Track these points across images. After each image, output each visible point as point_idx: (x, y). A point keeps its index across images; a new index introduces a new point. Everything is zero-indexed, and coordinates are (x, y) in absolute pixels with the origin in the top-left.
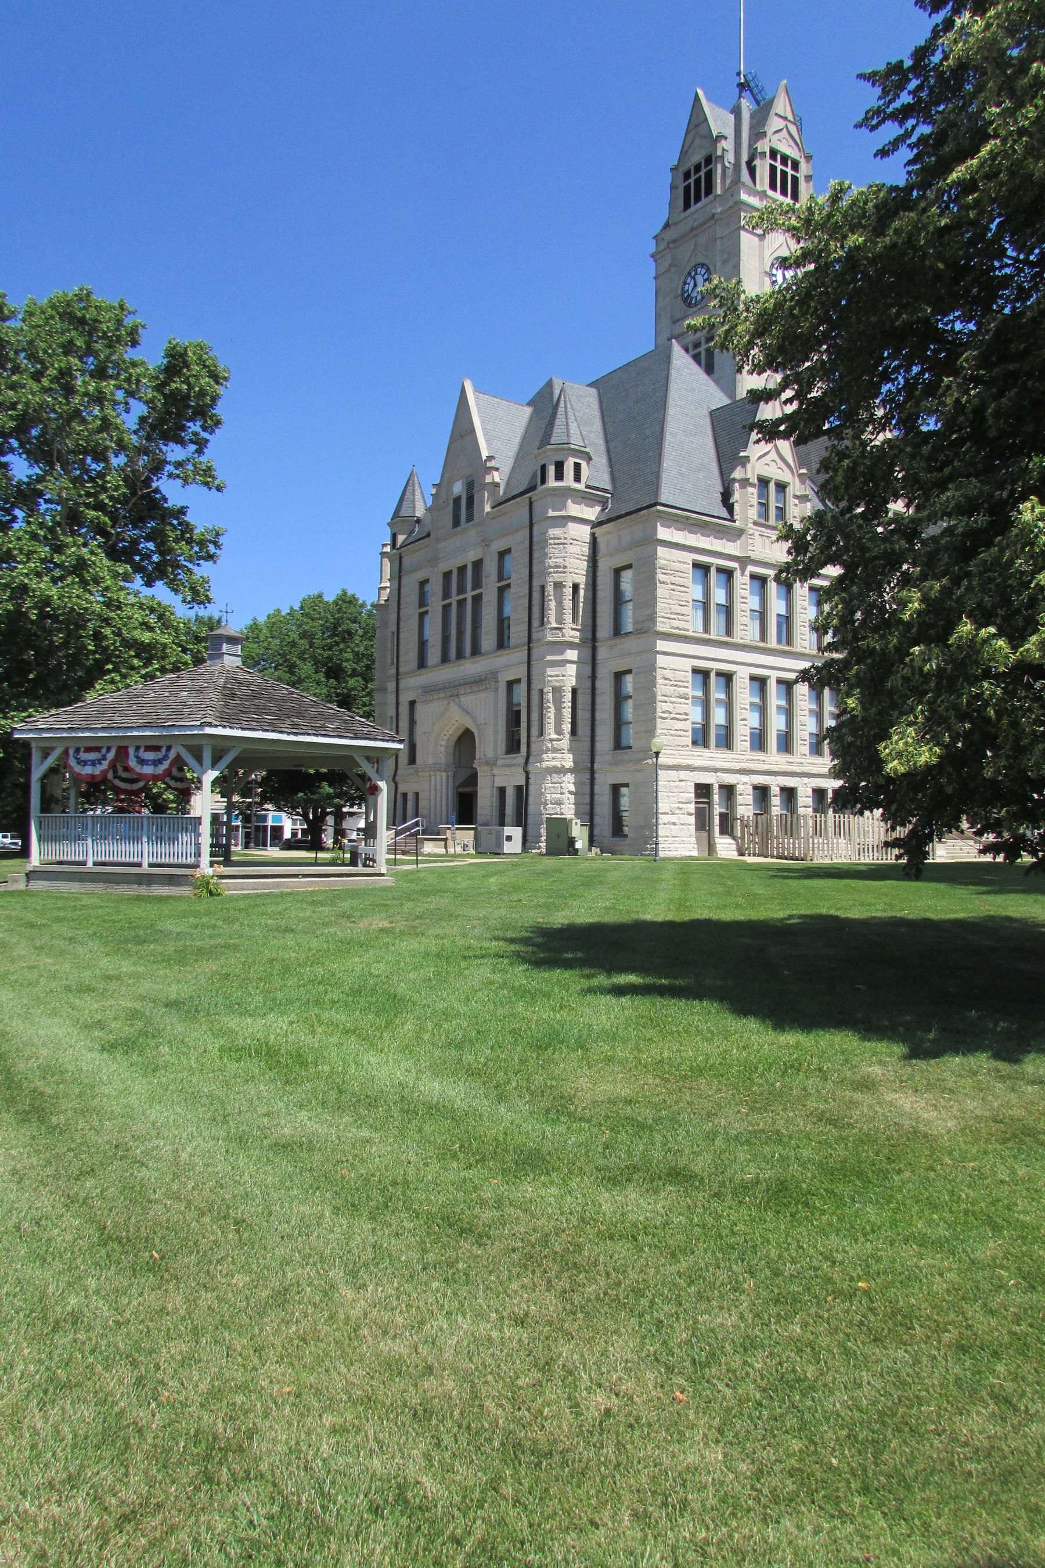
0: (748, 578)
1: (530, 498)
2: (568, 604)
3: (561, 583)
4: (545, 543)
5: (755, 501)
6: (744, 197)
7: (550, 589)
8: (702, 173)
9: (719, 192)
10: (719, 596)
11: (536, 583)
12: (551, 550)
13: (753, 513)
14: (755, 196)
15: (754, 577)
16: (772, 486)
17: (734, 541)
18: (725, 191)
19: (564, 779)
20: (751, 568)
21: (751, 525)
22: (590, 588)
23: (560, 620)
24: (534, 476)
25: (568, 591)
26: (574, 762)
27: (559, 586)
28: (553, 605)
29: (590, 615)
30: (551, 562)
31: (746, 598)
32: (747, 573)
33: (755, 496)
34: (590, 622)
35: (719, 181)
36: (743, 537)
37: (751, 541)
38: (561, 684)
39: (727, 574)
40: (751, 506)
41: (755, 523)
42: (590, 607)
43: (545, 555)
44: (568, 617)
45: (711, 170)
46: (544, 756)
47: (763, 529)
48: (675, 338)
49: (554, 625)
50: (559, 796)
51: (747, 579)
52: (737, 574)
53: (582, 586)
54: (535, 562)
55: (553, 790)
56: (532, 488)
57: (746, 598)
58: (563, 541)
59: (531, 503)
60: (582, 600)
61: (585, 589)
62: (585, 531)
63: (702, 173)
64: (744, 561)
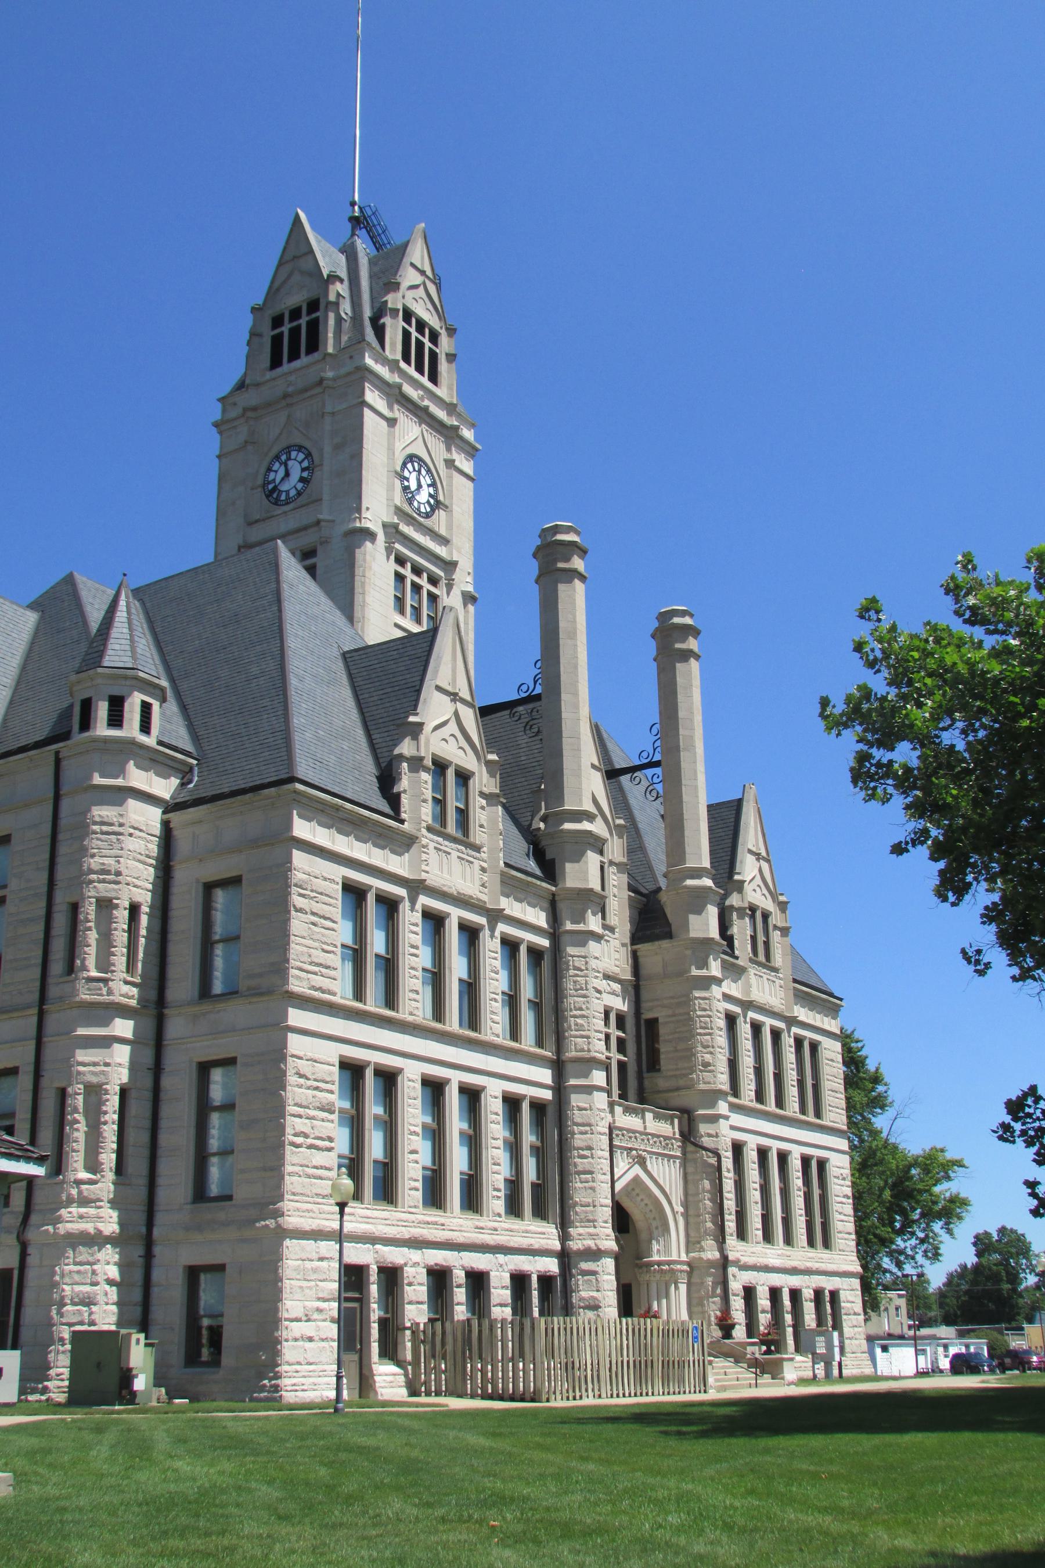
0: (420, 915)
1: (57, 753)
2: (121, 937)
3: (110, 900)
4: (83, 829)
5: (429, 794)
6: (369, 361)
7: (90, 909)
8: (303, 321)
9: (330, 350)
10: (377, 942)
11: (61, 899)
12: (94, 843)
13: (427, 812)
14: (383, 365)
15: (428, 915)
16: (450, 773)
17: (400, 854)
18: (341, 350)
19: (100, 1256)
20: (423, 900)
21: (424, 831)
22: (158, 913)
23: (105, 964)
24: (65, 715)
25: (122, 915)
26: (121, 1224)
27: (106, 905)
28: (93, 936)
29: (156, 961)
30: (95, 863)
31: (416, 947)
32: (418, 907)
33: (430, 786)
34: (154, 973)
35: (330, 335)
36: (415, 848)
37: (424, 856)
38: (102, 1079)
39: (390, 906)
40: (425, 801)
41: (429, 829)
42: (155, 947)
43: (83, 851)
44: (120, 961)
45: (317, 319)
46: (63, 1212)
47: (440, 840)
48: (282, 537)
49: (94, 973)
50: (87, 1288)
51: (417, 917)
52: (405, 907)
53: (145, 909)
54: (60, 860)
55: (77, 1278)
56: (60, 736)
57: (416, 947)
58: (116, 829)
59: (58, 762)
60: (143, 932)
61: (150, 915)
62: (151, 817)
63: (303, 321)
64: (416, 887)
